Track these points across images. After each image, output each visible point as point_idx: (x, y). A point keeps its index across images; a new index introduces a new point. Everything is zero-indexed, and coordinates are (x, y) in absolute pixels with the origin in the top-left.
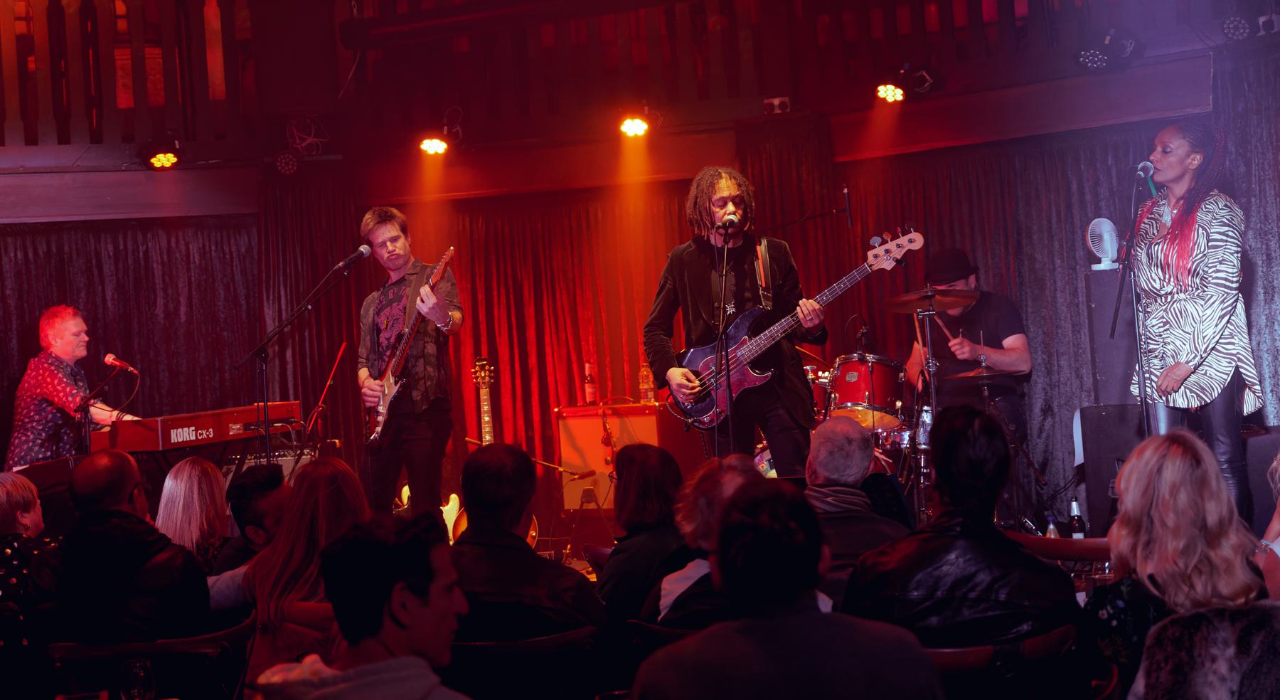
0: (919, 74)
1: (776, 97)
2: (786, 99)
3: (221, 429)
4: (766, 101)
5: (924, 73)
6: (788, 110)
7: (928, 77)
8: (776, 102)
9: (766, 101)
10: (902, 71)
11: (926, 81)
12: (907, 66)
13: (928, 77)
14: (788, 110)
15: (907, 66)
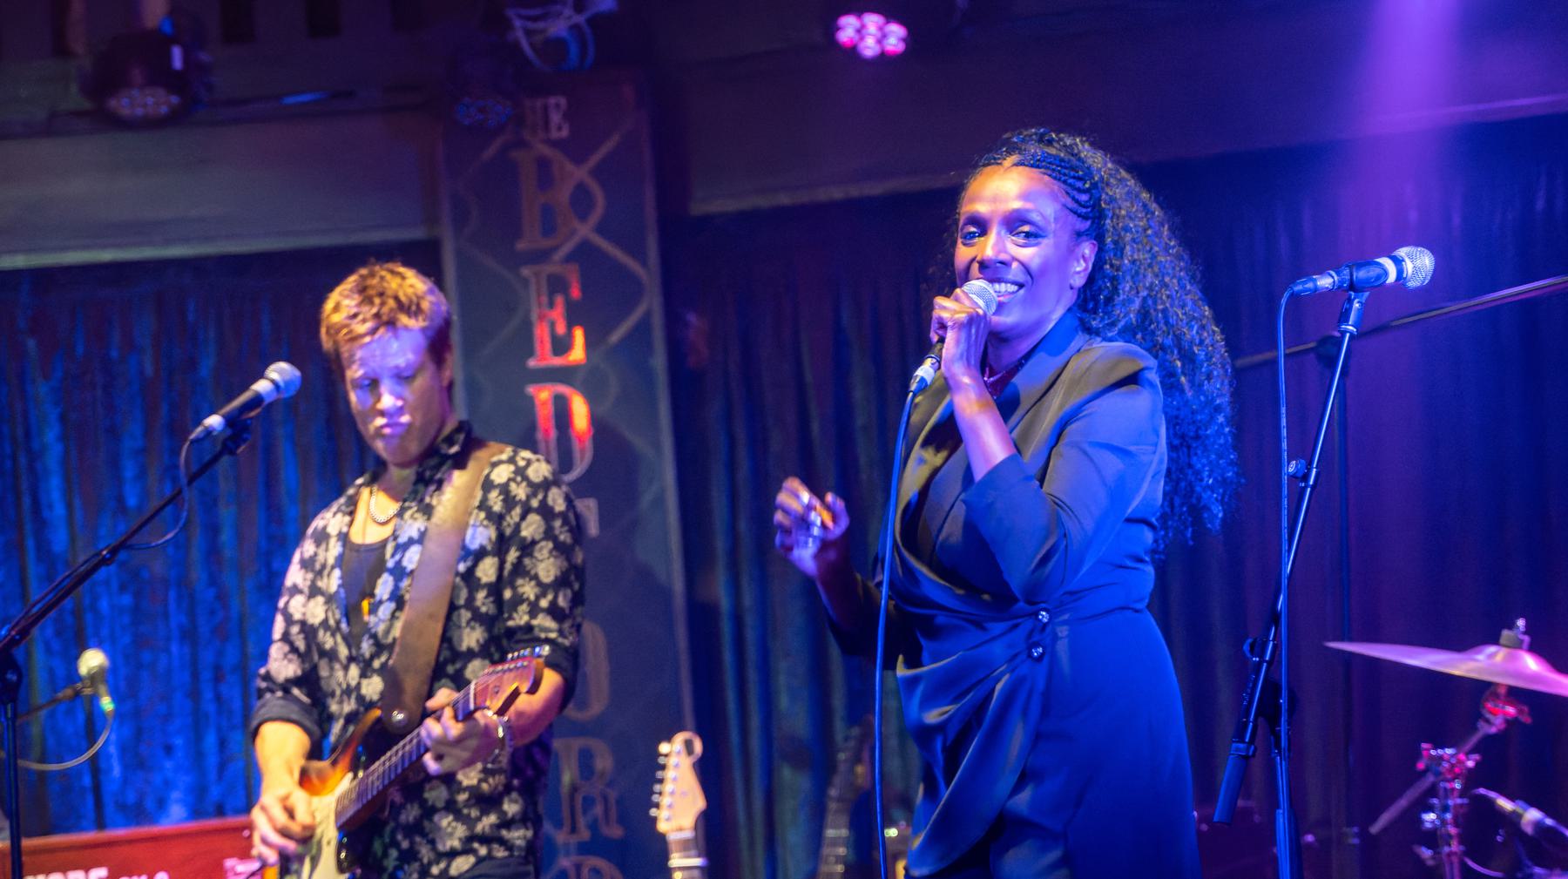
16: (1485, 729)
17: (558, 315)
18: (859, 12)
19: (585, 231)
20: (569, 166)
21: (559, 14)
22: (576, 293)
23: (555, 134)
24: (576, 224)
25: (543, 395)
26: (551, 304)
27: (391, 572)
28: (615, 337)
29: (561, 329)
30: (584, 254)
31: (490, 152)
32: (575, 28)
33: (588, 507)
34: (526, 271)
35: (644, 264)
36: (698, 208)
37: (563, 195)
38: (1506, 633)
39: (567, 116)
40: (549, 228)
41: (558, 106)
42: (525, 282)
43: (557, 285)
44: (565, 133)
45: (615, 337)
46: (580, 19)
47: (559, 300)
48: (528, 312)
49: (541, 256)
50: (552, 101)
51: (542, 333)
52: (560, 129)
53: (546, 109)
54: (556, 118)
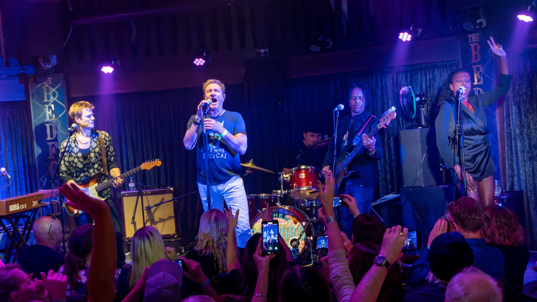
0: (327, 40)
1: (263, 49)
2: (267, 50)
3: (30, 204)
4: (258, 51)
5: (330, 40)
6: (268, 55)
7: (331, 42)
8: (262, 51)
9: (258, 51)
10: (320, 39)
11: (330, 43)
12: (322, 37)
13: (331, 42)
14: (268, 55)
15: (322, 37)
16: (246, 174)
17: (50, 112)
18: (106, 66)
19: (55, 99)
20: (52, 89)
21: (49, 64)
22: (53, 109)
23: (49, 83)
24: (54, 98)
25: (48, 126)
26: (49, 111)
27: (93, 152)
28: (60, 116)
29: (51, 114)
30: (54, 103)
31: (38, 86)
32: (52, 67)
33: (56, 143)
34: (45, 105)
35: (65, 105)
36: (72, 96)
37: (51, 94)
38: (250, 161)
39: (51, 81)
40: (49, 98)
41: (50, 79)
42: (45, 107)
43: (50, 108)
44: (51, 84)
45: (60, 116)
46: (53, 66)
47: (51, 110)
48: (45, 112)
49: (47, 103)
50: (49, 78)
51: (47, 115)
52: (50, 83)
53: (48, 79)
54: (50, 81)
